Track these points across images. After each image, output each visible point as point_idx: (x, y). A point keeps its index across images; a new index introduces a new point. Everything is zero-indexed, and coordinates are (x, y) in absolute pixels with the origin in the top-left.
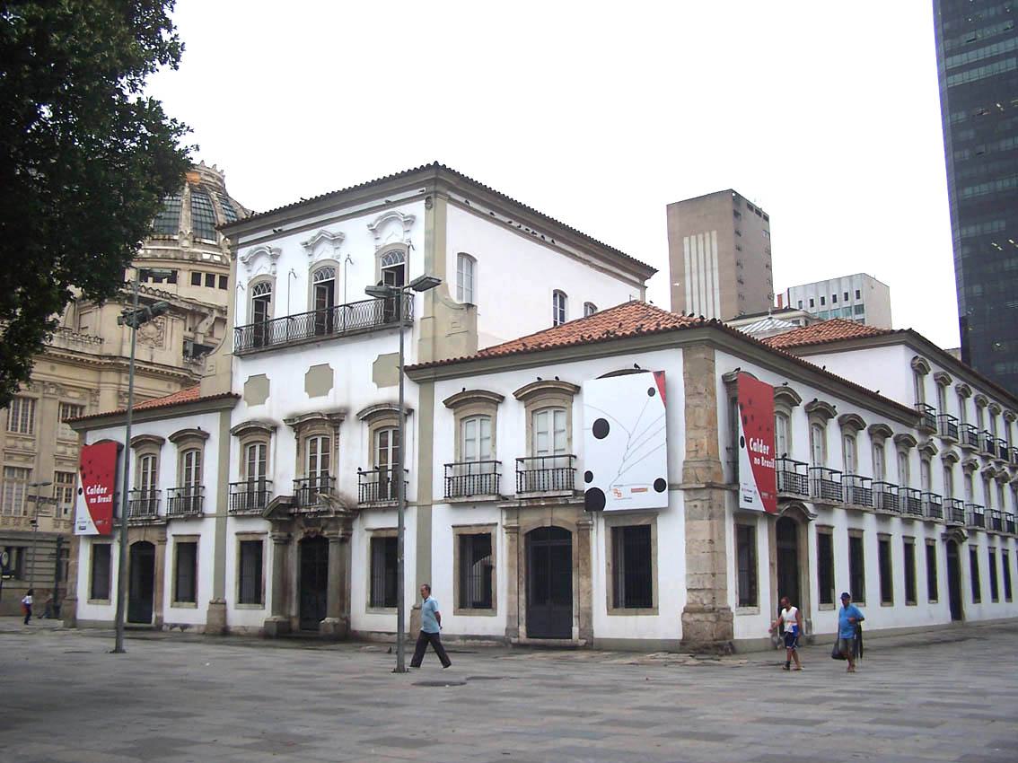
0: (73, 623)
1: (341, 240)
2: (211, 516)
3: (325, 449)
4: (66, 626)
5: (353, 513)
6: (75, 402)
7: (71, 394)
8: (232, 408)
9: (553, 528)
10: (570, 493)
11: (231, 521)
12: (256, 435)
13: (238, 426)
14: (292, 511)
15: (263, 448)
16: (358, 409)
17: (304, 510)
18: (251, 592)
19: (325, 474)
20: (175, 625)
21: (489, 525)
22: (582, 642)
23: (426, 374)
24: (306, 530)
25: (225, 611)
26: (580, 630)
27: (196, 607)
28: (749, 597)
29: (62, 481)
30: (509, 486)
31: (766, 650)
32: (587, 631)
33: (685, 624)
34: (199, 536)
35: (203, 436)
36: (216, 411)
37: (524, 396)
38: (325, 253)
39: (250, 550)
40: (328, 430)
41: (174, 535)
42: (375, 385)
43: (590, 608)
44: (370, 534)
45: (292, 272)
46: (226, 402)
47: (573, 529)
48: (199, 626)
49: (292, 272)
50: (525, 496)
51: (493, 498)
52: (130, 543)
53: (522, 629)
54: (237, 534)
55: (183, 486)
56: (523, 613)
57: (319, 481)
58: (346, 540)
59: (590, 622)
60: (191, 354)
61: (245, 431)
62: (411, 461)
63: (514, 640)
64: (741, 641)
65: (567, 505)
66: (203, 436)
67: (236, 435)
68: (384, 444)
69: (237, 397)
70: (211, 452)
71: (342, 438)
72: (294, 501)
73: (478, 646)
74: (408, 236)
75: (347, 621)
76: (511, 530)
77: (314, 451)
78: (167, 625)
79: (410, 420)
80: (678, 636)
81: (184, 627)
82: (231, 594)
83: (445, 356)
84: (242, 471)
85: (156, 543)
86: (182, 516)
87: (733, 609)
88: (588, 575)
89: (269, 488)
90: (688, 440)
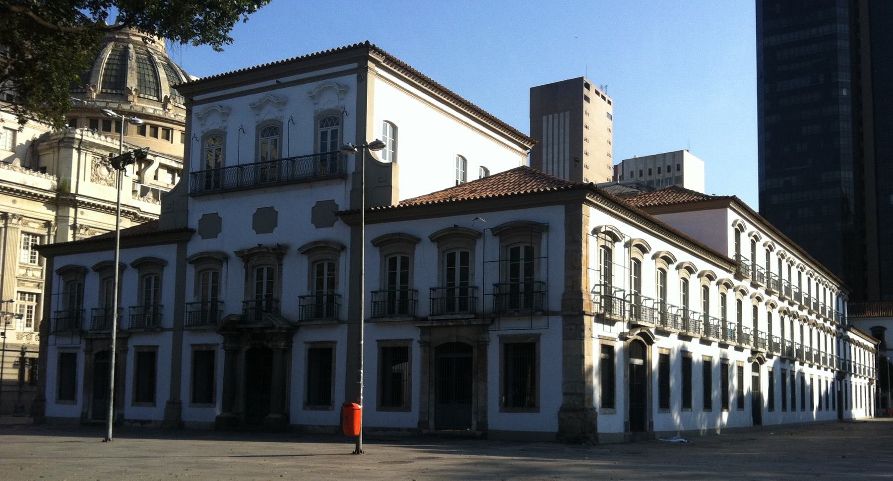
1: (284, 104)
2: (169, 330)
3: (270, 276)
5: (293, 328)
6: (35, 231)
7: (31, 224)
8: (189, 241)
10: (473, 316)
12: (211, 263)
13: (194, 256)
14: (242, 326)
15: (216, 276)
16: (300, 244)
17: (251, 326)
19: (269, 297)
20: (136, 421)
21: (406, 340)
22: (479, 433)
25: (180, 408)
26: (478, 423)
27: (155, 405)
29: (24, 299)
30: (424, 308)
31: (621, 443)
32: (483, 425)
33: (561, 420)
35: (161, 264)
36: (174, 243)
37: (436, 239)
39: (203, 358)
42: (313, 226)
43: (486, 407)
44: (309, 346)
45: (242, 128)
49: (242, 128)
50: (435, 318)
51: (411, 319)
52: (95, 352)
53: (432, 424)
54: (192, 345)
55: (144, 304)
56: (432, 409)
57: (264, 301)
58: (287, 350)
59: (486, 417)
60: (139, 193)
61: (201, 260)
62: (343, 287)
63: (425, 431)
64: (604, 435)
65: (469, 325)
66: (161, 264)
67: (191, 263)
68: (320, 273)
69: (192, 231)
70: (169, 277)
71: (285, 268)
72: (243, 319)
75: (287, 417)
77: (260, 277)
78: (129, 421)
79: (343, 254)
81: (143, 422)
82: (186, 394)
84: (195, 294)
87: (598, 410)
88: (485, 379)
89: (220, 308)
90: (566, 278)
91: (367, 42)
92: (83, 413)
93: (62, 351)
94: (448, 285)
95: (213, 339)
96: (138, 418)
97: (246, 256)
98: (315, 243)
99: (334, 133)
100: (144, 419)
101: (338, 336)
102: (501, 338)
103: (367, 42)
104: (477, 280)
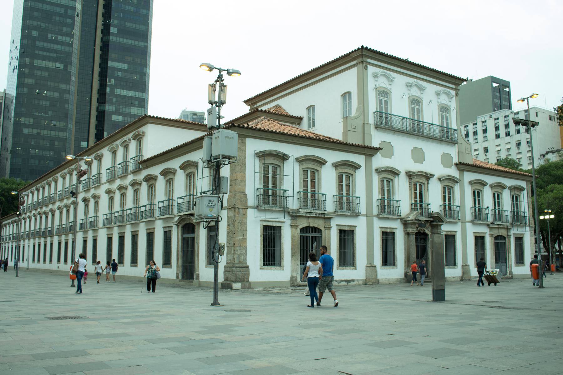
0: (247, 286)
4: (243, 287)
8: (373, 155)
9: (502, 236)
11: (375, 220)
18: (388, 259)
20: (342, 281)
23: (462, 166)
24: (419, 229)
27: (355, 269)
28: (167, 262)
32: (511, 273)
34: (356, 226)
38: (415, 92)
40: (424, 180)
41: (337, 225)
46: (370, 151)
47: (506, 237)
48: (362, 280)
52: (301, 227)
70: (360, 177)
73: (269, 288)
74: (390, 87)
76: (491, 235)
80: (363, 277)
81: (348, 281)
83: (351, 141)
85: (323, 229)
86: (349, 214)
91: (362, 46)
92: (292, 277)
93: (265, 224)
94: (339, 193)
95: (483, 230)
96: (343, 279)
97: (410, 175)
98: (449, 176)
99: (418, 110)
100: (350, 279)
101: (457, 229)
102: (514, 234)
103: (362, 46)
104: (505, 208)
